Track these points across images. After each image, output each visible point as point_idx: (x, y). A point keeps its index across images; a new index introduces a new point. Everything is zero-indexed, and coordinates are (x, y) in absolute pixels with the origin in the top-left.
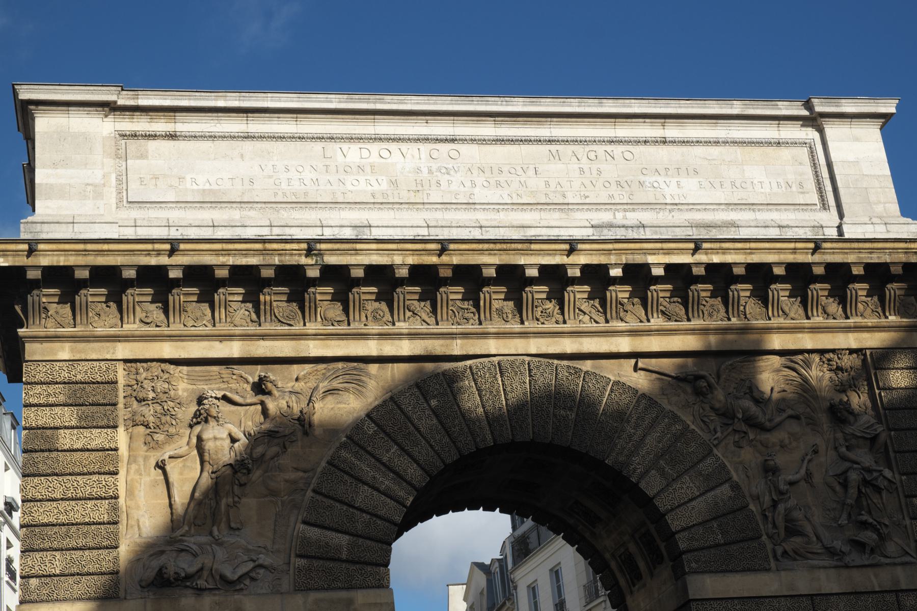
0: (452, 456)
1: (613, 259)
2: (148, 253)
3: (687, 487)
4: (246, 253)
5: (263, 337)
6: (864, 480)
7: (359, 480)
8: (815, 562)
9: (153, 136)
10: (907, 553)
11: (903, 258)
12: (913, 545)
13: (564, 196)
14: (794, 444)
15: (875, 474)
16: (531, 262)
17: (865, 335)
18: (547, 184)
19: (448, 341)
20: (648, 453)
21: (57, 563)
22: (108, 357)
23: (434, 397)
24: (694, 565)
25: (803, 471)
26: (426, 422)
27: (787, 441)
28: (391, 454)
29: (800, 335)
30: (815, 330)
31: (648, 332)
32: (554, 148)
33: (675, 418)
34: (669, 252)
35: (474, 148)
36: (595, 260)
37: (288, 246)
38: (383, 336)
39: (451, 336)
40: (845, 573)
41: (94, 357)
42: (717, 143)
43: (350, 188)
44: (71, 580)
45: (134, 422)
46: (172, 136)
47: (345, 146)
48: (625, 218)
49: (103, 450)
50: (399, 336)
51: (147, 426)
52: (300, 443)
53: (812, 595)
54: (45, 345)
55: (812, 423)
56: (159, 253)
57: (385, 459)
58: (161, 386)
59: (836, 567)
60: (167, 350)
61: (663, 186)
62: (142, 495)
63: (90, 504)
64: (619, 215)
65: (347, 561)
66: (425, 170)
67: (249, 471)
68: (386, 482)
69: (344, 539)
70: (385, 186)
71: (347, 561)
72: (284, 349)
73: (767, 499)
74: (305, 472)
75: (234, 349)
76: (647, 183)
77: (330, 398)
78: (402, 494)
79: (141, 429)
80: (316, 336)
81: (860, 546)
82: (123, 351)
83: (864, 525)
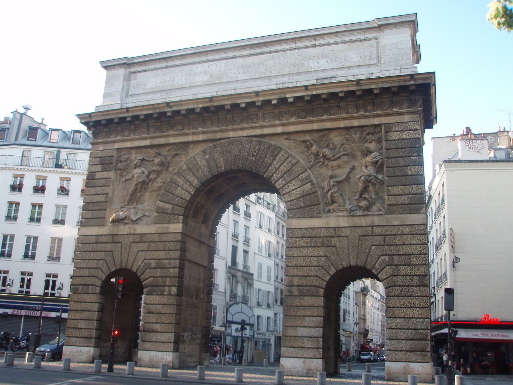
0: (209, 176)
1: (273, 97)
2: (121, 113)
3: (293, 184)
4: (149, 109)
5: (156, 137)
6: (367, 180)
7: (178, 186)
8: (339, 214)
9: (139, 72)
10: (381, 210)
11: (397, 84)
12: (386, 206)
13: (271, 73)
14: (345, 166)
15: (372, 177)
16: (242, 102)
17: (382, 118)
18: (266, 69)
19: (215, 134)
20: (280, 172)
21: (90, 214)
22: (112, 148)
23: (207, 154)
24: (290, 215)
25: (344, 177)
26: (202, 163)
27: (341, 165)
28: (190, 176)
29: (353, 121)
30: (359, 118)
31: (289, 124)
32: (271, 55)
33: (294, 157)
34: (295, 92)
35: (242, 59)
36: (266, 98)
37: (160, 106)
38: (193, 134)
39: (216, 132)
40: (351, 219)
41: (108, 148)
42: (337, 43)
43: (196, 80)
44: (93, 220)
45: (116, 170)
46: (145, 71)
47: (197, 65)
48: (293, 79)
49: (106, 178)
50: (198, 133)
51: (121, 170)
52: (164, 174)
53: (335, 228)
54: (97, 146)
55: (354, 156)
56: (124, 113)
57: (187, 178)
58: (126, 156)
59: (348, 216)
60: (128, 144)
61: (311, 64)
62: (116, 193)
63: (100, 196)
64: (291, 78)
65: (170, 214)
66: (223, 70)
67: (148, 184)
68: (186, 186)
69: (170, 206)
70: (208, 78)
71: (170, 214)
72: (162, 141)
73: (326, 189)
74: (164, 183)
75: (147, 143)
76: (305, 64)
77: (176, 157)
78: (191, 190)
79: (119, 172)
80: (172, 136)
81: (360, 207)
82: (117, 146)
83: (365, 199)
